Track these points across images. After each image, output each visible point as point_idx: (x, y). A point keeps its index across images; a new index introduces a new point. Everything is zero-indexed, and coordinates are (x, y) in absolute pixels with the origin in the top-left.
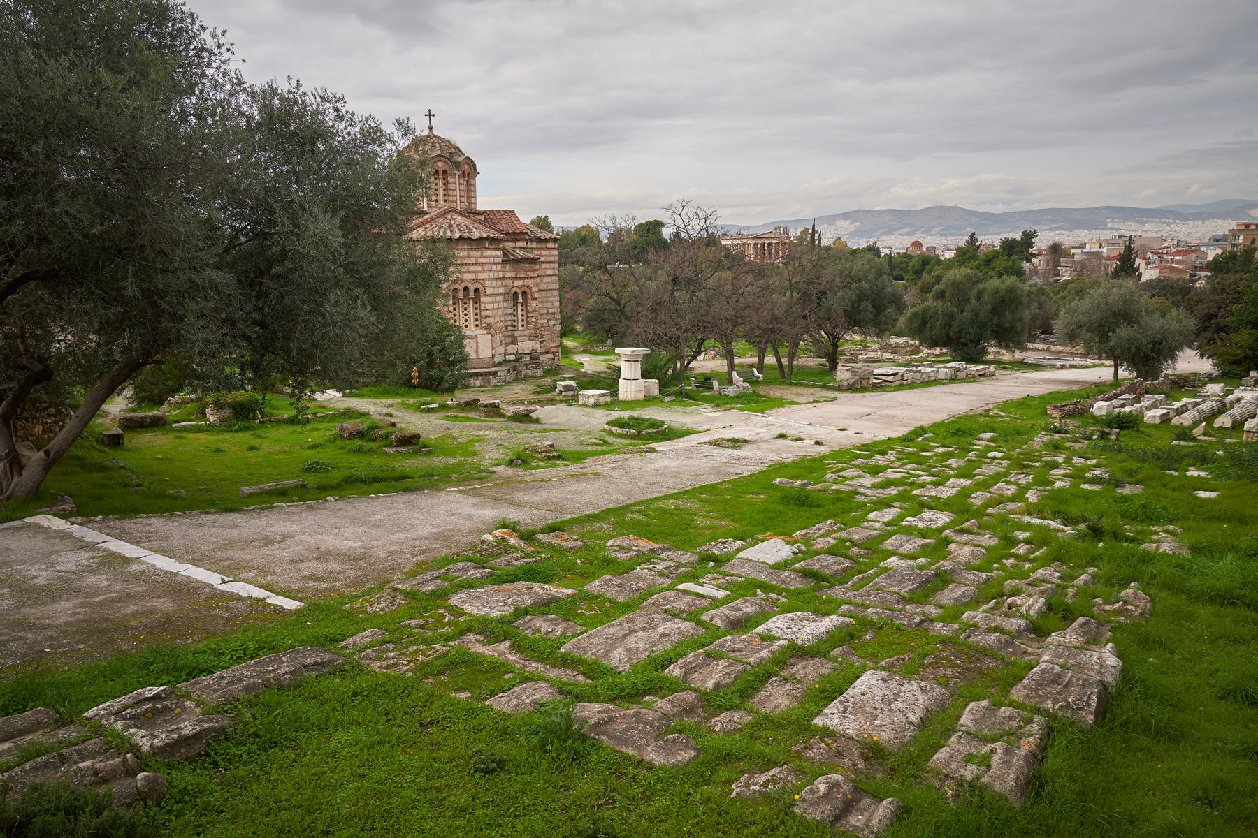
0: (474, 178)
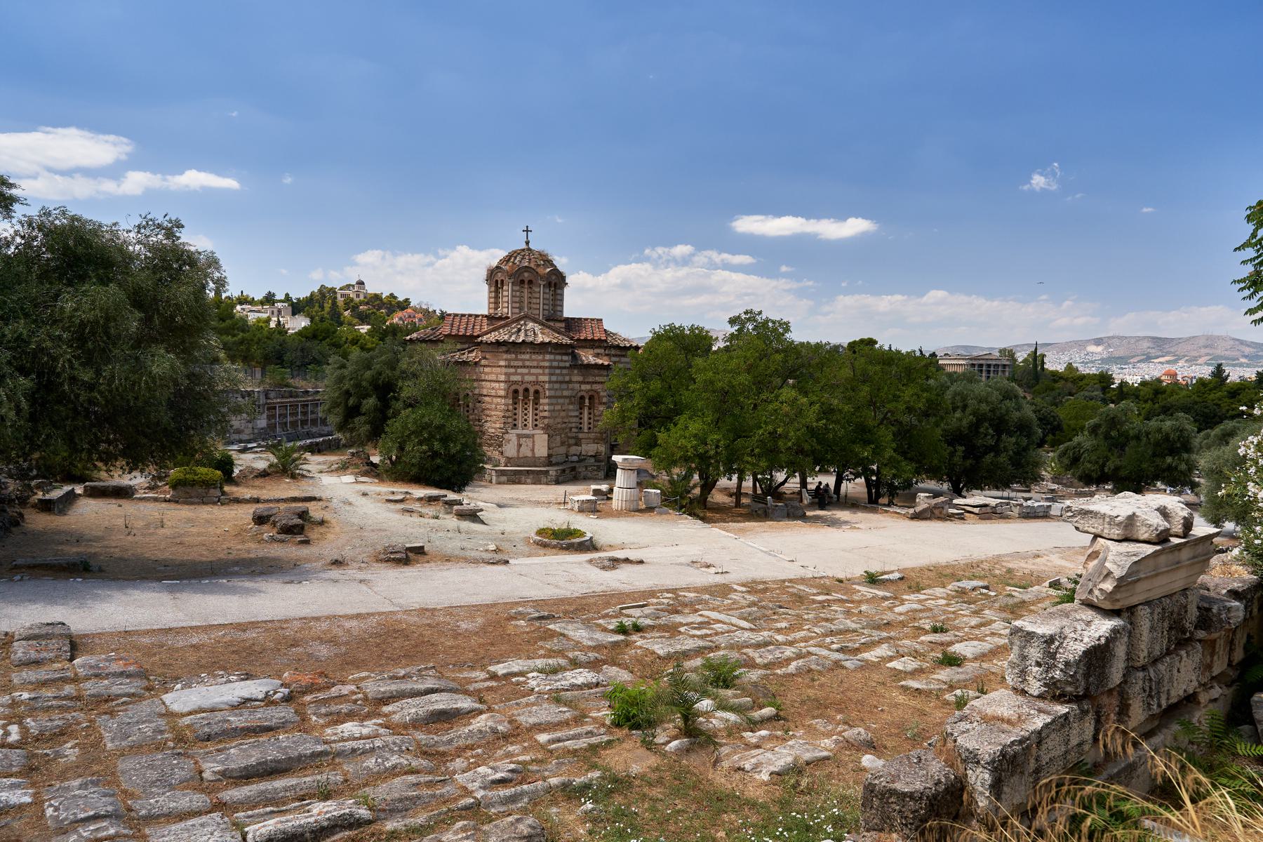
0: (562, 289)
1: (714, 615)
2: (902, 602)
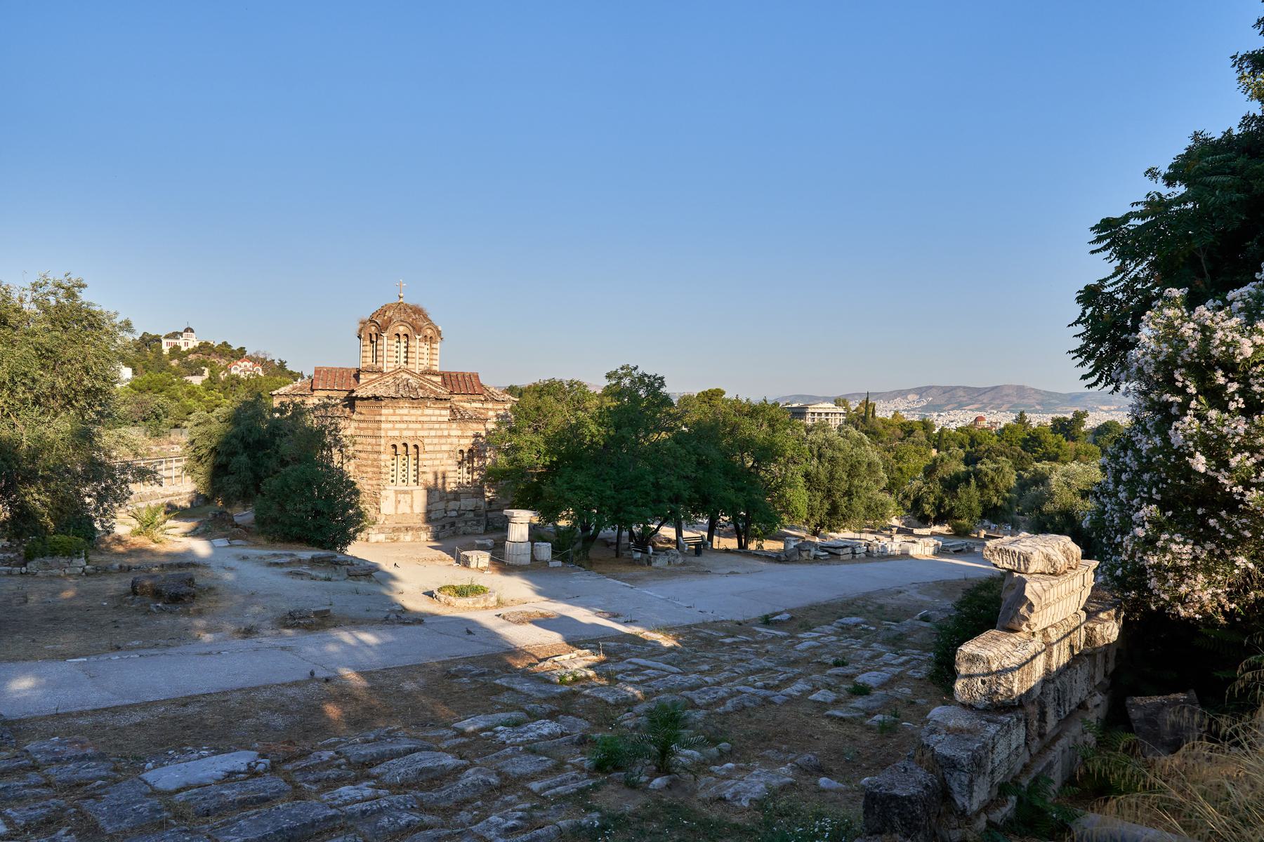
1: (642, 661)
2: (800, 641)
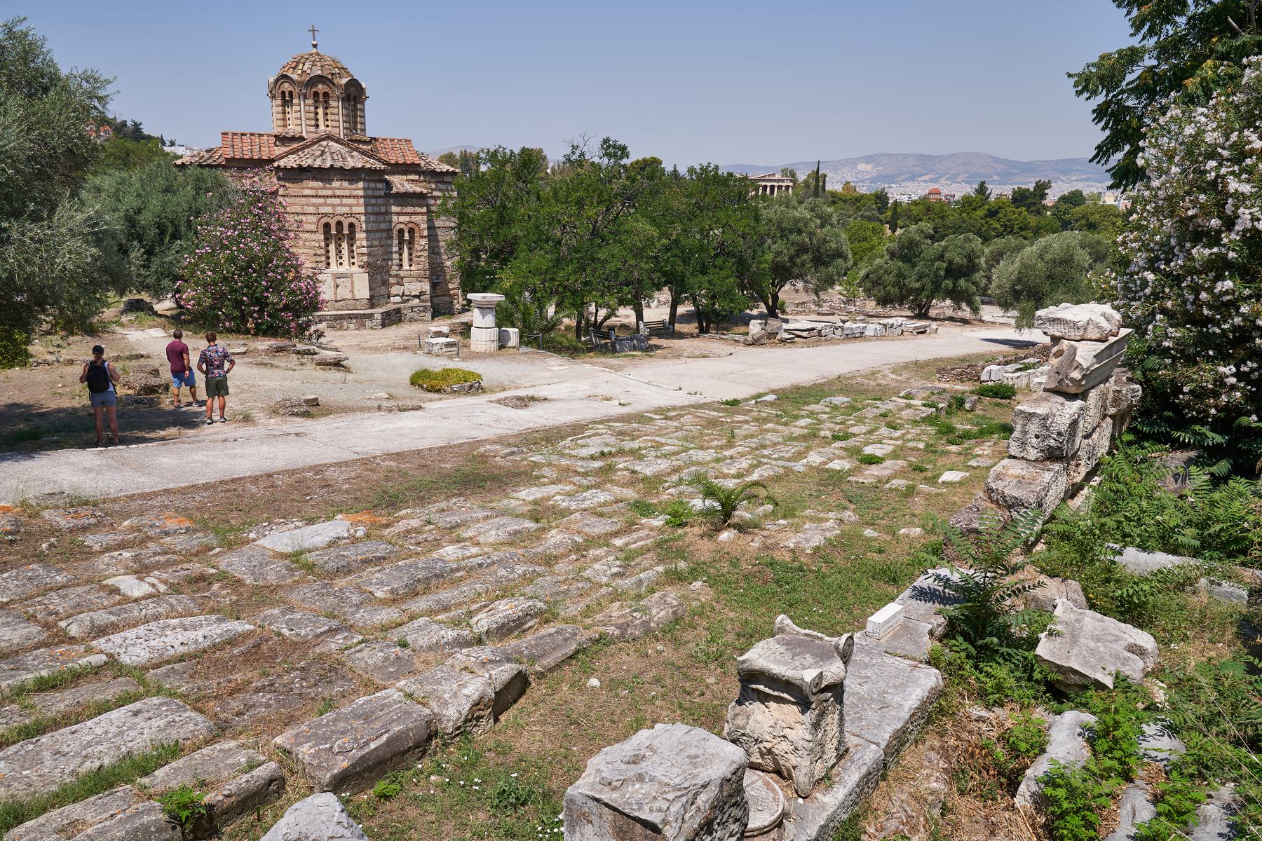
0: (363, 103)
